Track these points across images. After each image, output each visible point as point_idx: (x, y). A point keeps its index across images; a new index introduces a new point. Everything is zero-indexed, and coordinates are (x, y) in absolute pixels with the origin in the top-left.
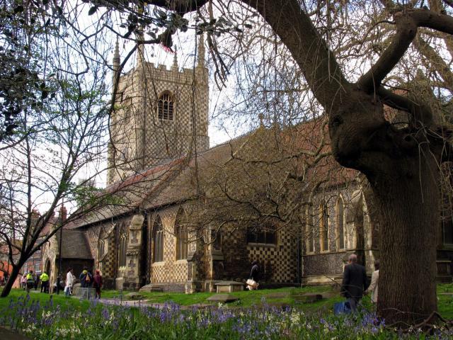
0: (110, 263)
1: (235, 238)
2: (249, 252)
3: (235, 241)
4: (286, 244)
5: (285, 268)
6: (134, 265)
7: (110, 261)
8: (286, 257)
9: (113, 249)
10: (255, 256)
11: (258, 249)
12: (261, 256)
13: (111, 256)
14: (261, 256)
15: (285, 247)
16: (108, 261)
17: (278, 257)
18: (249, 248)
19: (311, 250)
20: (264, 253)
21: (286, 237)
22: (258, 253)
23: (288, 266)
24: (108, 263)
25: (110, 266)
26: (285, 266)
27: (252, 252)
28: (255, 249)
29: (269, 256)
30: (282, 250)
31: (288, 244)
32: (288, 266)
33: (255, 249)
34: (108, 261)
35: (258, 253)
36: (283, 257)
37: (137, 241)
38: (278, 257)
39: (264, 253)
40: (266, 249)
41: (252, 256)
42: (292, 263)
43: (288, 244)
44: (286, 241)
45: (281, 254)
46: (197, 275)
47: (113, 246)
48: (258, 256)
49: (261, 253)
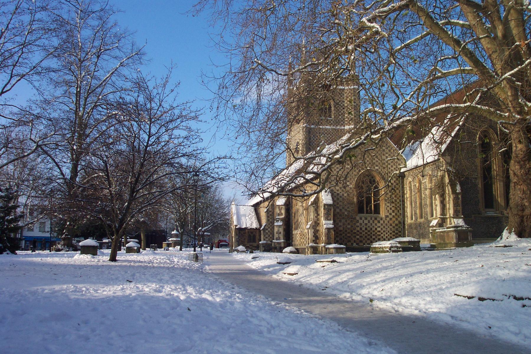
0: (269, 231)
1: (346, 210)
2: (358, 221)
3: (346, 213)
4: (391, 214)
5: (391, 234)
6: (280, 233)
7: (269, 229)
8: (391, 225)
9: (270, 220)
10: (363, 224)
11: (366, 219)
12: (369, 224)
13: (269, 226)
14: (369, 224)
15: (391, 217)
16: (267, 229)
17: (384, 225)
18: (358, 218)
19: (412, 219)
20: (371, 222)
21: (391, 209)
22: (366, 222)
23: (394, 232)
24: (267, 231)
25: (269, 233)
26: (390, 232)
27: (361, 221)
28: (363, 219)
29: (376, 225)
30: (388, 219)
31: (393, 214)
32: (394, 232)
33: (363, 219)
34: (267, 229)
35: (366, 222)
36: (389, 224)
37: (282, 214)
38: (384, 225)
39: (371, 222)
40: (373, 219)
41: (361, 224)
42: (397, 229)
43: (393, 214)
44: (391, 211)
45: (386, 222)
46: (313, 241)
47: (358, 221)
48: (366, 224)
49: (369, 222)
